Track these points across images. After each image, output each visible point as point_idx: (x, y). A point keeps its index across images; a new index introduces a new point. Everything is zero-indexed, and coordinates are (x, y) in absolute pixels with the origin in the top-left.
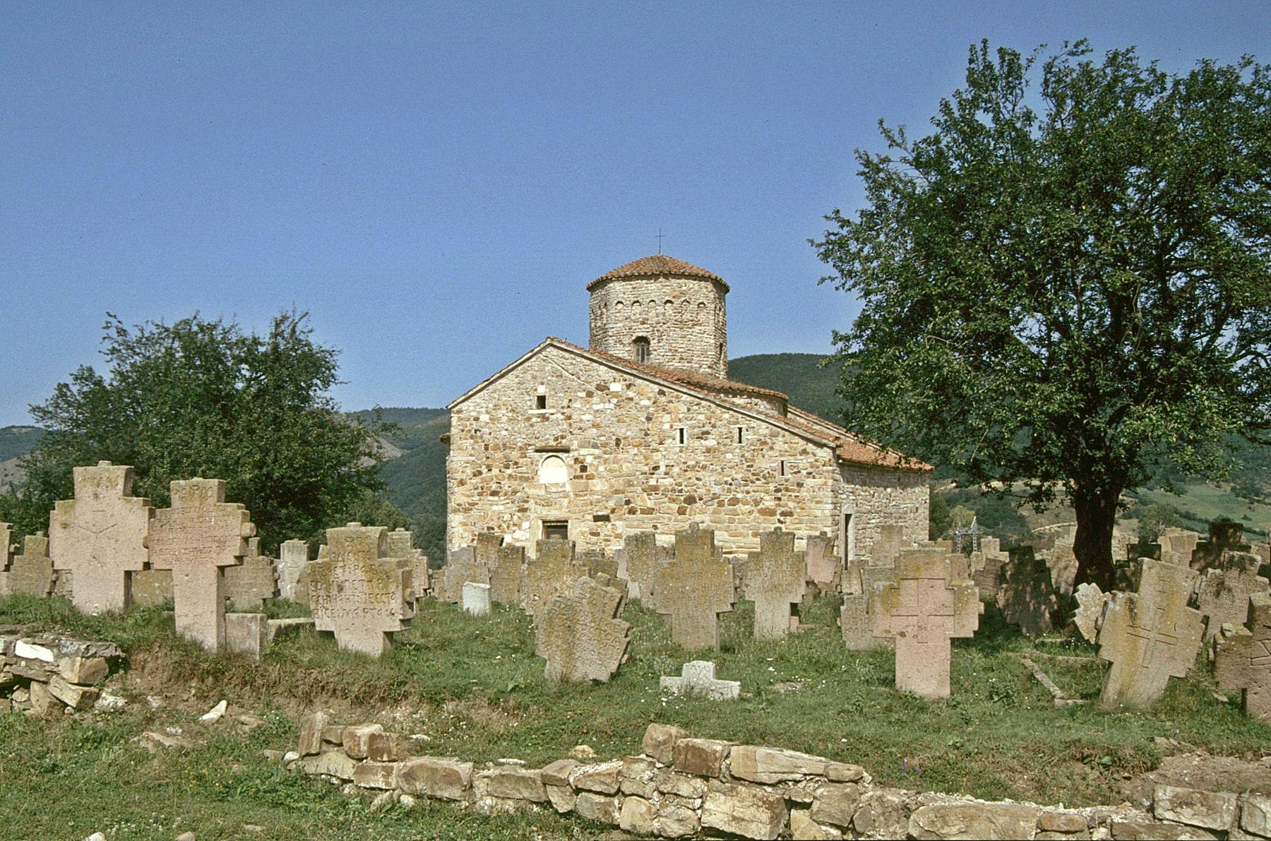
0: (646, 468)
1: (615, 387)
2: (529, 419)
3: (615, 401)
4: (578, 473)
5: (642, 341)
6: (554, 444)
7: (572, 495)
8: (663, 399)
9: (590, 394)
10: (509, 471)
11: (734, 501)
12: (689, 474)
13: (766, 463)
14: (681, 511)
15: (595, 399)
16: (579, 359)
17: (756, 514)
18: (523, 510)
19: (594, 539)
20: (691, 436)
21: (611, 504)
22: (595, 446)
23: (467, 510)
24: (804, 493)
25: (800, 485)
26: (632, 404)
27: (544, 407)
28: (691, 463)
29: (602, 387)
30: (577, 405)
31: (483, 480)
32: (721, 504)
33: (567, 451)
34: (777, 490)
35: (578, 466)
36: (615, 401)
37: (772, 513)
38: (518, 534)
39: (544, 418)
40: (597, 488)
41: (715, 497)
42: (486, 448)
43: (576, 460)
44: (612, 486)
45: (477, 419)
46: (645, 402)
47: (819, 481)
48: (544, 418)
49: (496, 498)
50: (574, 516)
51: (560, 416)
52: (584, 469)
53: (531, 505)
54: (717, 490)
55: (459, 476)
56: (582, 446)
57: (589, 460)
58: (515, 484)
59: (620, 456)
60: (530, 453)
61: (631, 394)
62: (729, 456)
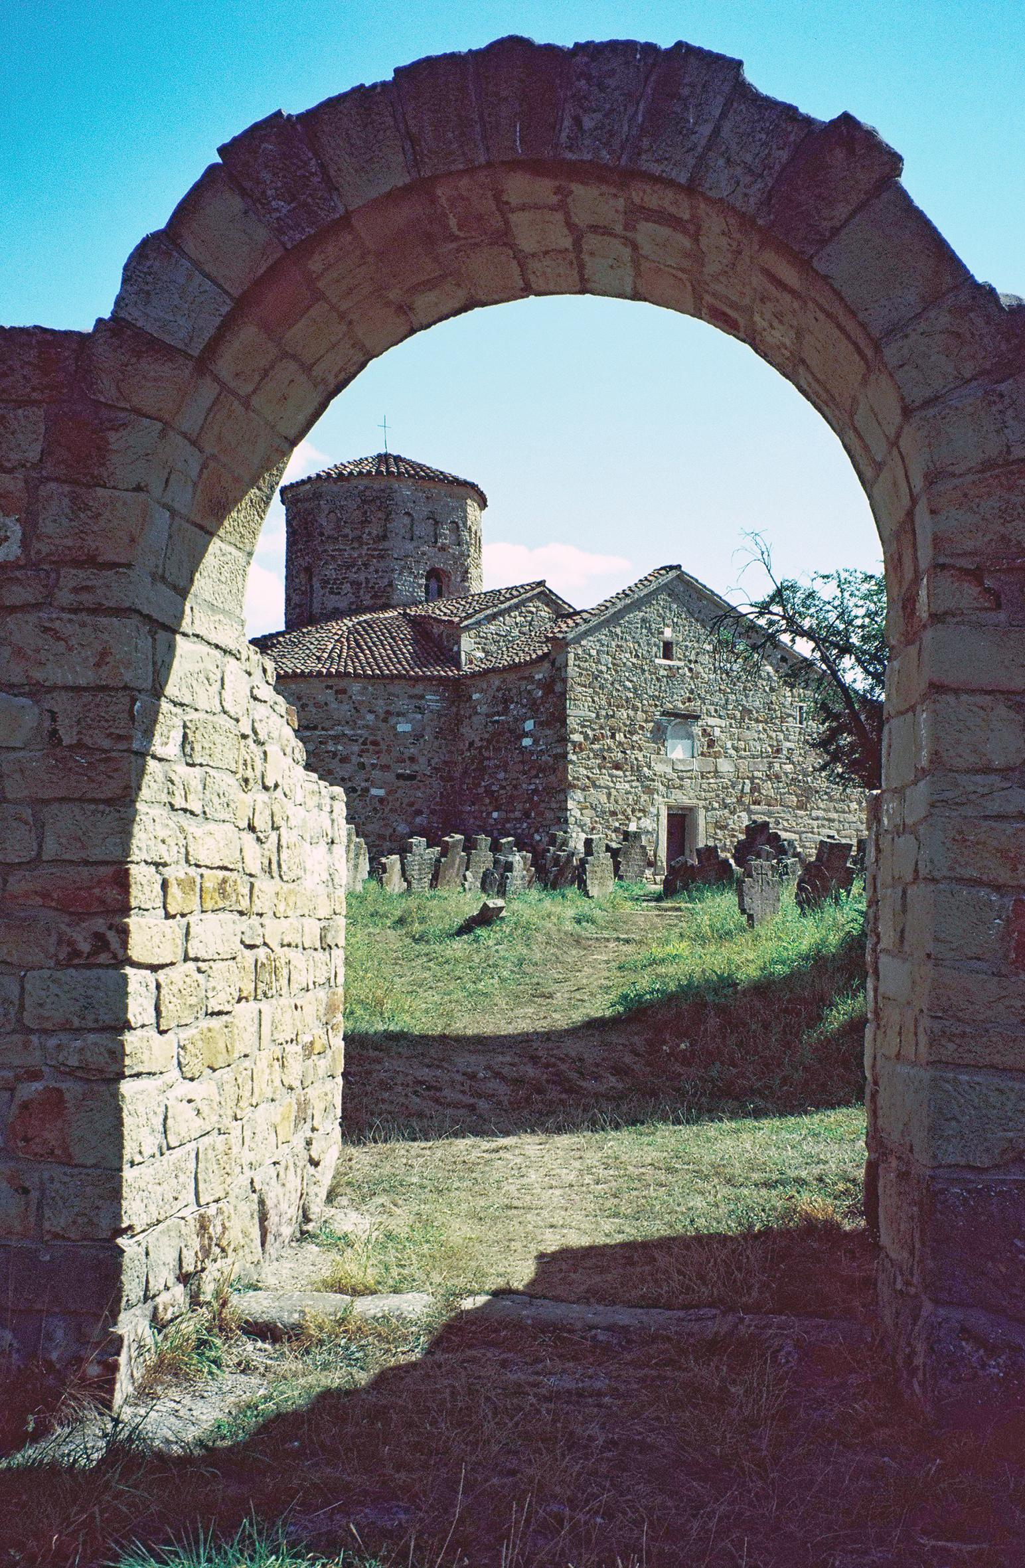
10: (635, 738)
35: (705, 740)
49: (620, 773)
50: (701, 803)
52: (711, 744)
55: (576, 737)
57: (717, 732)
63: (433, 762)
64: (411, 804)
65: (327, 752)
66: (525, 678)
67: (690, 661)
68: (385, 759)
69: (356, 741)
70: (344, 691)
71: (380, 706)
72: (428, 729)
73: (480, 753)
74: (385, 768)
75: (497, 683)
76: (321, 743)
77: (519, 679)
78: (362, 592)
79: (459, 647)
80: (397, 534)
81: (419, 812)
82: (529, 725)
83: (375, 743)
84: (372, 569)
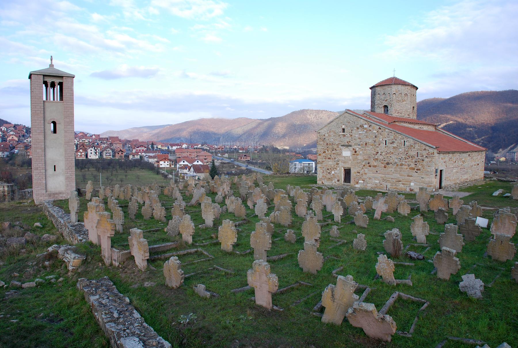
0: (375, 153)
1: (365, 126)
2: (339, 136)
5: (386, 107)
8: (380, 130)
9: (358, 128)
10: (333, 152)
11: (402, 165)
12: (388, 155)
13: (413, 153)
14: (385, 167)
15: (359, 130)
17: (408, 169)
18: (338, 164)
19: (358, 174)
20: (388, 143)
21: (364, 163)
23: (321, 163)
24: (424, 163)
26: (370, 132)
28: (389, 152)
29: (362, 126)
31: (326, 154)
32: (397, 165)
34: (416, 162)
37: (414, 169)
38: (336, 171)
39: (344, 136)
40: (360, 158)
41: (396, 163)
47: (429, 159)
48: (344, 136)
52: (356, 152)
53: (340, 163)
54: (396, 161)
56: (355, 144)
57: (357, 149)
58: (335, 156)
59: (367, 148)
60: (340, 146)
61: (370, 129)
62: (400, 150)
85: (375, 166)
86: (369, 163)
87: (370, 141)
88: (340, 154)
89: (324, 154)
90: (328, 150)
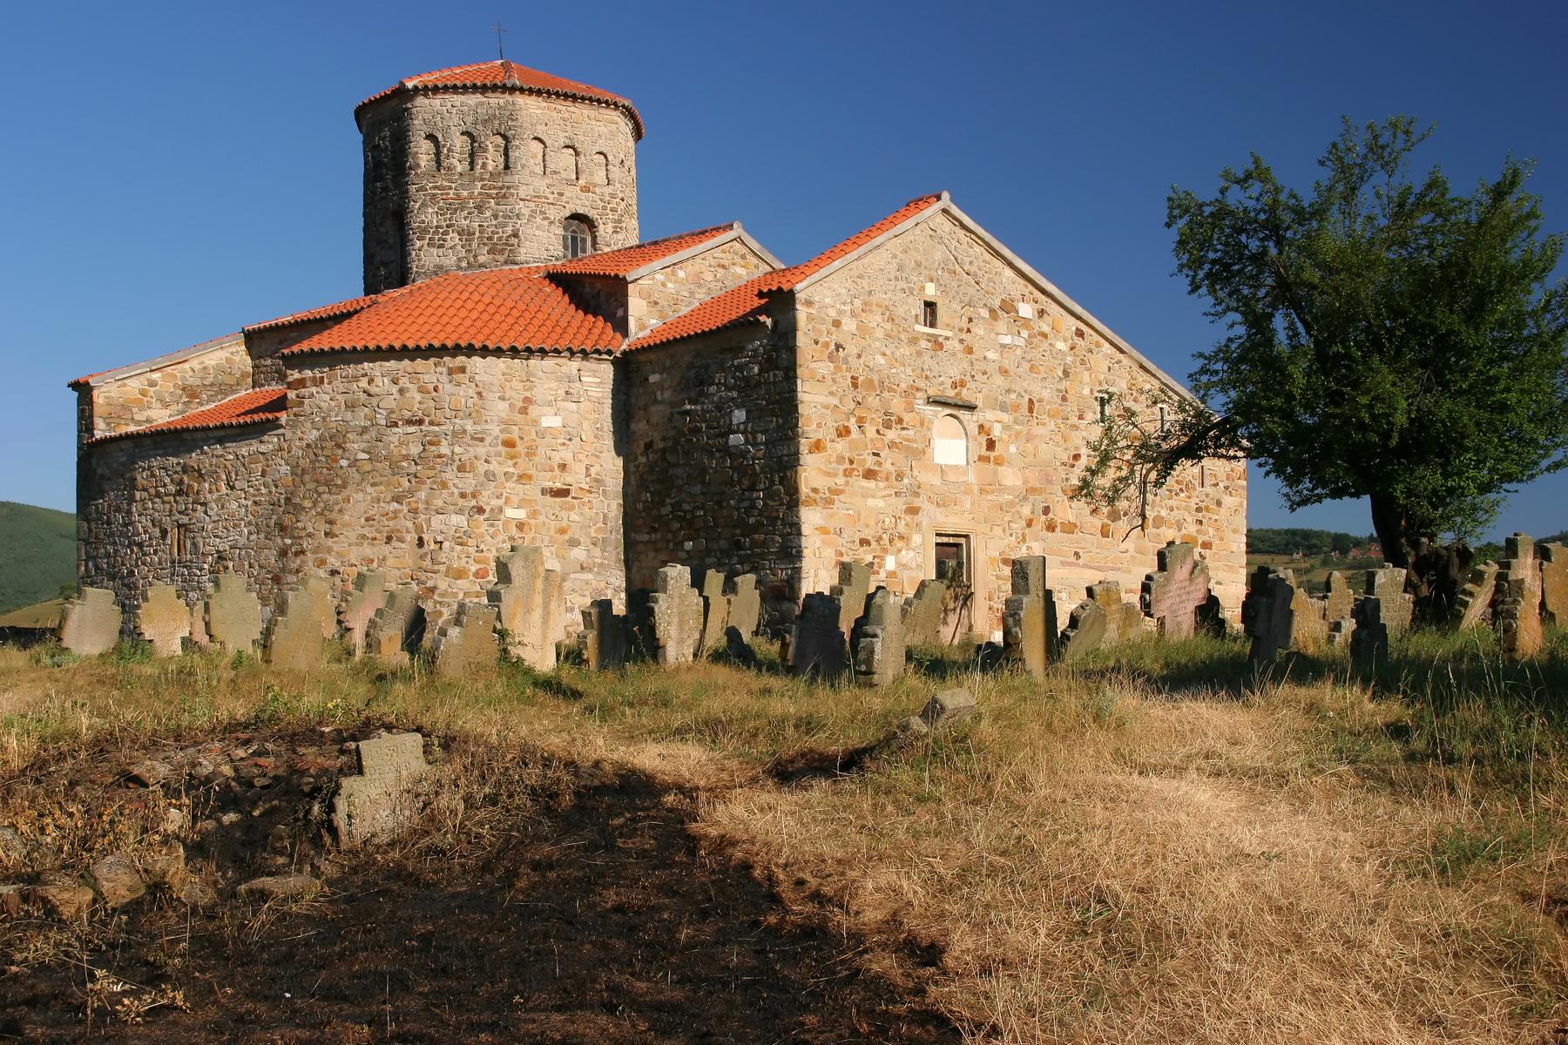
3: (1025, 333)
4: (984, 452)
6: (951, 393)
7: (976, 491)
10: (891, 435)
15: (1001, 326)
16: (978, 249)
21: (1026, 511)
22: (1003, 408)
25: (1219, 503)
26: (1045, 345)
27: (932, 325)
30: (979, 330)
33: (971, 408)
34: (1199, 510)
35: (983, 439)
36: (1025, 333)
38: (907, 556)
39: (938, 345)
42: (855, 386)
43: (981, 427)
44: (1025, 482)
45: (837, 324)
46: (1061, 345)
49: (871, 484)
51: (957, 344)
52: (991, 445)
57: (997, 432)
59: (1038, 430)
61: (1046, 329)
63: (593, 471)
64: (563, 531)
65: (440, 456)
66: (731, 350)
67: (961, 330)
68: (524, 465)
69: (482, 440)
70: (463, 370)
71: (516, 391)
72: (586, 425)
73: (664, 459)
74: (524, 478)
75: (687, 358)
76: (431, 443)
77: (723, 351)
78: (475, 244)
79: (626, 311)
80: (523, 166)
81: (574, 543)
82: (739, 415)
83: (509, 444)
84: (488, 214)
85: (1070, 528)
86: (1046, 510)
87: (1045, 393)
88: (919, 453)
89: (841, 446)
90: (861, 422)
